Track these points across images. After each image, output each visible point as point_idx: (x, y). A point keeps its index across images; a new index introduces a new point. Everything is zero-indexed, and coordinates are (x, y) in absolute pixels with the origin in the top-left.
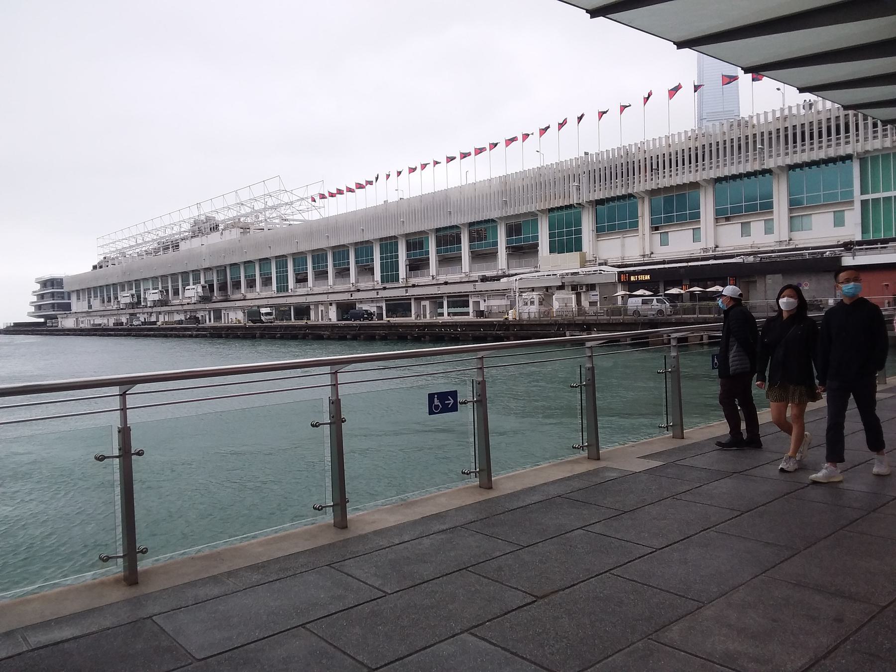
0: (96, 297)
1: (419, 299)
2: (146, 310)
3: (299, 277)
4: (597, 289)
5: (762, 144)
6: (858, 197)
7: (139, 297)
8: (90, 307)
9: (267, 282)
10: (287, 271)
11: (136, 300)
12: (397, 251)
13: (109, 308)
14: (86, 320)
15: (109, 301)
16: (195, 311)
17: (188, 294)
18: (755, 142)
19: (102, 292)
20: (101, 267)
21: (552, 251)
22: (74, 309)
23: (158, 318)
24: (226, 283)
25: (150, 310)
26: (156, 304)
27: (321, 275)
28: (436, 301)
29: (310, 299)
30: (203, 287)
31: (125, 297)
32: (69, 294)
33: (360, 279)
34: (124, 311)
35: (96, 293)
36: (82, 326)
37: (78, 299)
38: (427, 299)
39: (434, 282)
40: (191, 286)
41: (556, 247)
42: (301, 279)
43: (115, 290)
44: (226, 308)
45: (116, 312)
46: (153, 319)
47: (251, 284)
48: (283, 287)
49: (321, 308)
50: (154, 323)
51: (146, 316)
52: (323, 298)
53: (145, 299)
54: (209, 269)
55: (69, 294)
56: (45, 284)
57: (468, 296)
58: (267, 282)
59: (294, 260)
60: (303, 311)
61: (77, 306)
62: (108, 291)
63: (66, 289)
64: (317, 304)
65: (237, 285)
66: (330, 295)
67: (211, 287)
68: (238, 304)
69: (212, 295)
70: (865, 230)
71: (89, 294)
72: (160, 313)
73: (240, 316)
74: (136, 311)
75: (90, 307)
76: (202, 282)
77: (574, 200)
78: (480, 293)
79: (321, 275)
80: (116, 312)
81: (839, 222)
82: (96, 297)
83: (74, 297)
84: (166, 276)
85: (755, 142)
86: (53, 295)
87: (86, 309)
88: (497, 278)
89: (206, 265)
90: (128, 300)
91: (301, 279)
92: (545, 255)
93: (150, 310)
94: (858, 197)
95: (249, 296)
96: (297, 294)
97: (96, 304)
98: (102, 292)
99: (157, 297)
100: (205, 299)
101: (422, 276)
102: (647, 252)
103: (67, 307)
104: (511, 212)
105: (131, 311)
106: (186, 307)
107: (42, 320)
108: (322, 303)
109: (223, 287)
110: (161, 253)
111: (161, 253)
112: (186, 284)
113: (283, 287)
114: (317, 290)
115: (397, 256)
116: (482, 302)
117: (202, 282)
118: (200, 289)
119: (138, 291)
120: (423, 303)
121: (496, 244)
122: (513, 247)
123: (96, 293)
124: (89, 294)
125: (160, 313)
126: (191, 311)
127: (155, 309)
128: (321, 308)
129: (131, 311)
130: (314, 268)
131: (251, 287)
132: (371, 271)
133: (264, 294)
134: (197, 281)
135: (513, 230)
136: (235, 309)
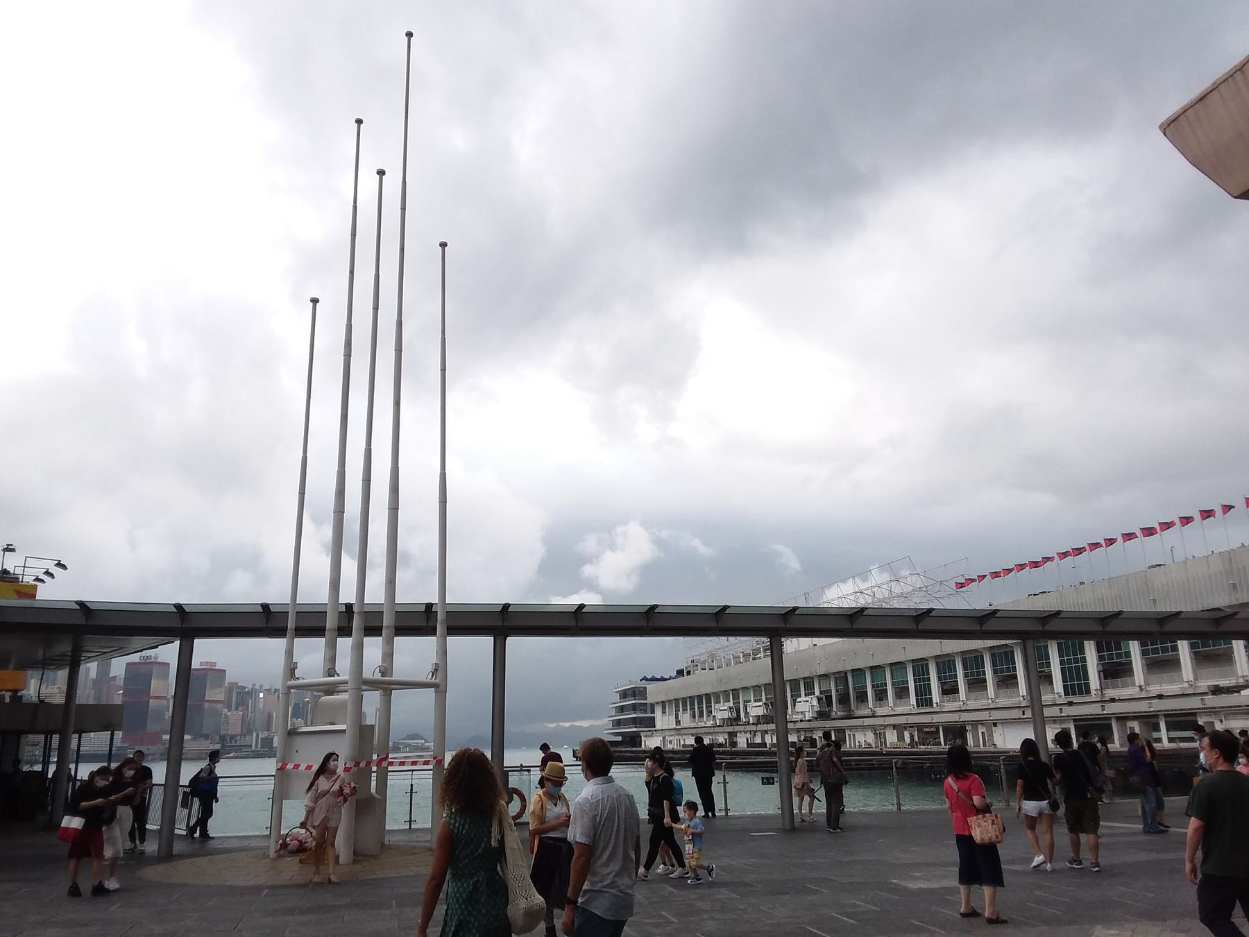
0: (685, 710)
2: (748, 728)
7: (738, 711)
8: (678, 722)
9: (902, 693)
10: (929, 679)
11: (735, 715)
13: (702, 724)
14: (674, 739)
15: (701, 715)
16: (811, 730)
17: (799, 707)
19: (692, 704)
20: (689, 673)
22: (659, 725)
23: (763, 738)
24: (848, 694)
25: (754, 728)
26: (760, 720)
27: (977, 683)
29: (965, 717)
30: (819, 699)
31: (721, 711)
32: (653, 706)
34: (721, 729)
35: (684, 705)
36: (670, 747)
37: (664, 712)
40: (803, 698)
42: (949, 690)
43: (708, 702)
44: (851, 728)
45: (712, 730)
46: (758, 740)
47: (881, 696)
48: (924, 699)
49: (981, 729)
50: (759, 745)
51: (748, 735)
52: (984, 716)
53: (746, 713)
54: (824, 677)
55: (653, 706)
56: (624, 695)
58: (902, 693)
59: (937, 664)
60: (956, 732)
61: (663, 721)
62: (700, 703)
63: (650, 700)
64: (975, 724)
65: (862, 697)
66: (993, 712)
67: (829, 698)
68: (867, 722)
69: (831, 710)
71: (677, 706)
72: (766, 732)
73: (870, 738)
74: (737, 728)
75: (678, 722)
76: (817, 692)
79: (977, 683)
80: (712, 730)
82: (685, 710)
83: (658, 710)
84: (747, 688)
86: (634, 708)
87: (673, 726)
89: (822, 671)
90: (726, 715)
91: (949, 690)
93: (754, 728)
95: (879, 711)
96: (945, 709)
97: (686, 719)
98: (692, 704)
99: (761, 711)
100: (822, 715)
101: (1125, 685)
103: (651, 722)
105: (730, 729)
106: (799, 725)
107: (620, 739)
108: (982, 723)
109: (844, 699)
110: (762, 655)
111: (762, 655)
112: (795, 696)
113: (924, 699)
114: (973, 704)
115: (1084, 659)
117: (817, 692)
118: (815, 702)
119: (736, 702)
123: (684, 705)
124: (677, 706)
125: (766, 732)
126: (806, 730)
127: (760, 727)
128: (981, 729)
129: (730, 729)
130: (966, 675)
131: (881, 699)
132: (1049, 679)
133: (899, 710)
134: (809, 691)
136: (863, 728)
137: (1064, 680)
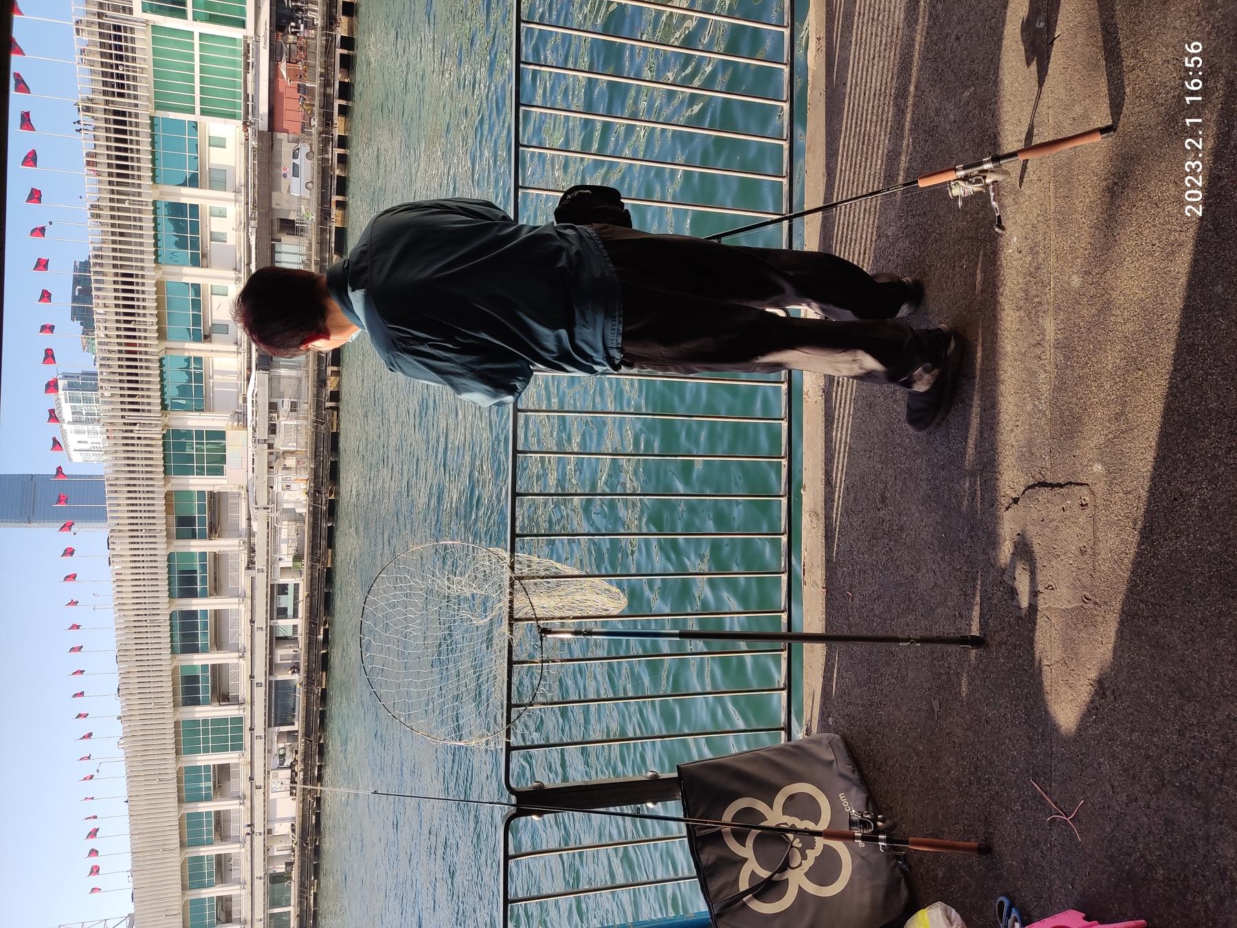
1: (272, 667)
3: (223, 918)
4: (274, 400)
5: (123, 201)
6: (196, 117)
12: (196, 722)
18: (119, 209)
21: (219, 471)
28: (276, 640)
33: (233, 833)
38: (271, 653)
39: (248, 655)
41: (217, 466)
57: (272, 586)
70: (233, 116)
77: (157, 433)
78: (270, 563)
81: (220, 143)
85: (119, 209)
88: (252, 550)
92: (225, 482)
94: (196, 117)
102: (234, 348)
104: (160, 525)
115: (205, 722)
116: (282, 564)
120: (278, 660)
121: (203, 555)
122: (210, 531)
135: (185, 526)
137: (225, 749)
